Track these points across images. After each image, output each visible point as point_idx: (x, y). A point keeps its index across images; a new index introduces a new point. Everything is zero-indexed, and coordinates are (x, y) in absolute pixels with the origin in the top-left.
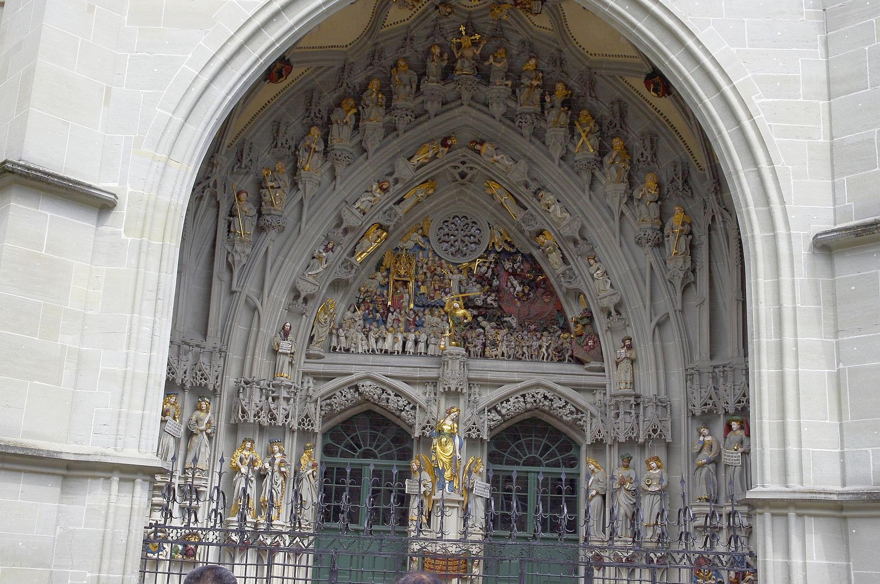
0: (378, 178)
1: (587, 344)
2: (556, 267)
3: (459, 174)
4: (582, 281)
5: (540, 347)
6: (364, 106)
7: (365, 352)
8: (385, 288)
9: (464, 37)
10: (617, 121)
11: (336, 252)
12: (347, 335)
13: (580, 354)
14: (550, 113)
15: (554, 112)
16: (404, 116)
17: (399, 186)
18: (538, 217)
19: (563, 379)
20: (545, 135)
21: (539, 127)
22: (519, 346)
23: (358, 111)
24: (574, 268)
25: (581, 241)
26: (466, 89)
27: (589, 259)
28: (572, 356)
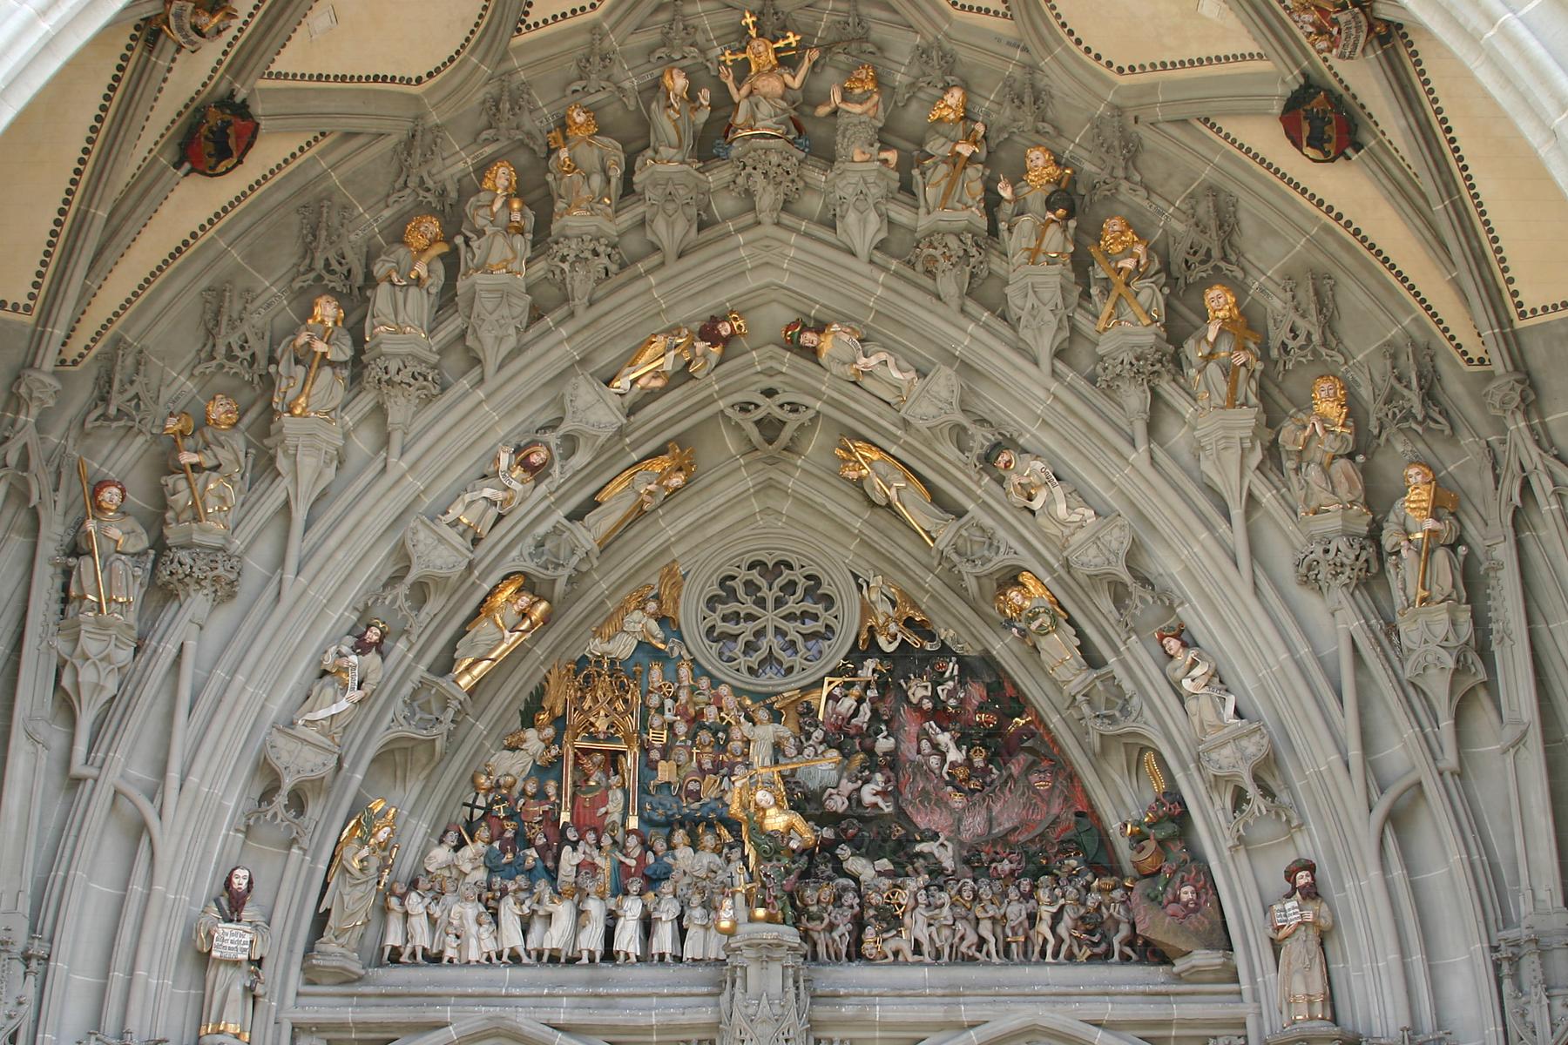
0: (514, 441)
1: (1177, 899)
2: (1061, 674)
3: (758, 423)
4: (1146, 709)
5: (1032, 918)
6: (469, 234)
7: (489, 959)
8: (554, 773)
9: (755, 43)
10: (1212, 241)
11: (392, 659)
12: (436, 911)
13: (1156, 926)
14: (1015, 230)
15: (1026, 222)
16: (588, 254)
17: (580, 459)
18: (1001, 533)
19: (1109, 1010)
20: (1008, 290)
21: (985, 273)
22: (965, 918)
23: (455, 250)
24: (1119, 672)
25: (1134, 587)
26: (765, 174)
27: (1162, 638)
28: (1130, 942)
